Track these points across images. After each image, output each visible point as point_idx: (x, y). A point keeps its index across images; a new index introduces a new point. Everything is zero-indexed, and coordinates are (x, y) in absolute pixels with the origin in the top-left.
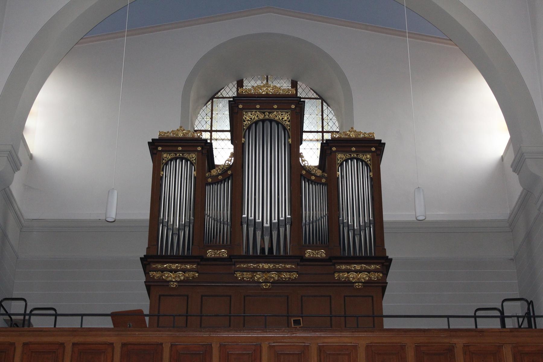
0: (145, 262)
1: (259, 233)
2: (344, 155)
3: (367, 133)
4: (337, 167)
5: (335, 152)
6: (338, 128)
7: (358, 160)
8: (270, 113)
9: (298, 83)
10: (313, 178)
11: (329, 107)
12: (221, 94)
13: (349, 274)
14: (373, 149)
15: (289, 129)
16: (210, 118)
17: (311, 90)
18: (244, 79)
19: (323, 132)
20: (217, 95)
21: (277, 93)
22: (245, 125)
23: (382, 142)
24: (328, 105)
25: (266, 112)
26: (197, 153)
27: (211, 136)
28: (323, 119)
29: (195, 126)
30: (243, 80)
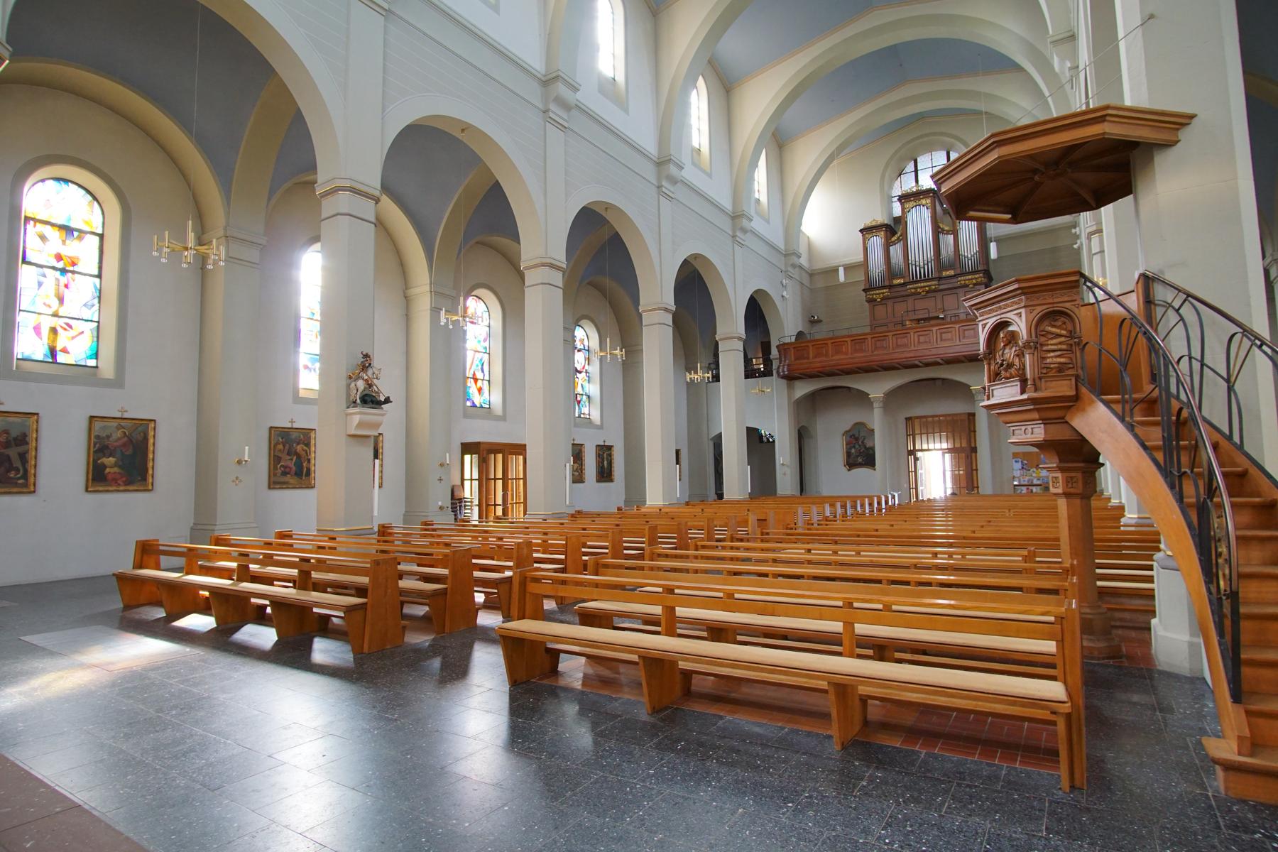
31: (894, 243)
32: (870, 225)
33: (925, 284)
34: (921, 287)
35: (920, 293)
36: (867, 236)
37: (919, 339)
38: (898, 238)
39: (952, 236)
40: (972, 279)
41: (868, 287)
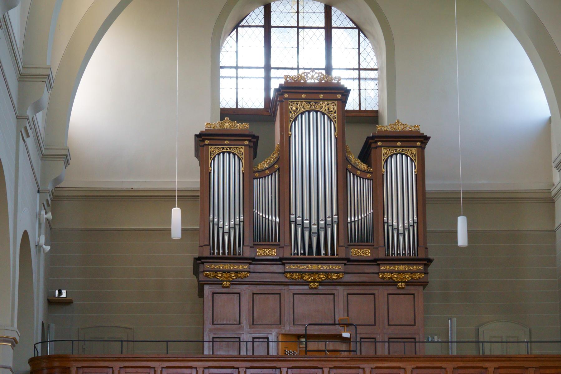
1: (307, 234)
2: (390, 150)
4: (383, 163)
5: (381, 146)
6: (377, 64)
7: (402, 154)
8: (316, 103)
9: (332, 8)
10: (359, 173)
11: (366, 39)
12: (247, 21)
14: (418, 144)
15: (335, 121)
17: (347, 18)
18: (272, 3)
19: (359, 69)
20: (242, 23)
21: (322, 80)
22: (291, 116)
23: (428, 136)
24: (365, 36)
25: (312, 102)
26: (244, 147)
27: (237, 73)
28: (359, 54)
30: (270, 4)
31: (262, 174)
33: (320, 267)
34: (312, 273)
35: (307, 283)
36: (211, 149)
38: (271, 167)
39: (370, 182)
40: (404, 272)
41: (206, 254)
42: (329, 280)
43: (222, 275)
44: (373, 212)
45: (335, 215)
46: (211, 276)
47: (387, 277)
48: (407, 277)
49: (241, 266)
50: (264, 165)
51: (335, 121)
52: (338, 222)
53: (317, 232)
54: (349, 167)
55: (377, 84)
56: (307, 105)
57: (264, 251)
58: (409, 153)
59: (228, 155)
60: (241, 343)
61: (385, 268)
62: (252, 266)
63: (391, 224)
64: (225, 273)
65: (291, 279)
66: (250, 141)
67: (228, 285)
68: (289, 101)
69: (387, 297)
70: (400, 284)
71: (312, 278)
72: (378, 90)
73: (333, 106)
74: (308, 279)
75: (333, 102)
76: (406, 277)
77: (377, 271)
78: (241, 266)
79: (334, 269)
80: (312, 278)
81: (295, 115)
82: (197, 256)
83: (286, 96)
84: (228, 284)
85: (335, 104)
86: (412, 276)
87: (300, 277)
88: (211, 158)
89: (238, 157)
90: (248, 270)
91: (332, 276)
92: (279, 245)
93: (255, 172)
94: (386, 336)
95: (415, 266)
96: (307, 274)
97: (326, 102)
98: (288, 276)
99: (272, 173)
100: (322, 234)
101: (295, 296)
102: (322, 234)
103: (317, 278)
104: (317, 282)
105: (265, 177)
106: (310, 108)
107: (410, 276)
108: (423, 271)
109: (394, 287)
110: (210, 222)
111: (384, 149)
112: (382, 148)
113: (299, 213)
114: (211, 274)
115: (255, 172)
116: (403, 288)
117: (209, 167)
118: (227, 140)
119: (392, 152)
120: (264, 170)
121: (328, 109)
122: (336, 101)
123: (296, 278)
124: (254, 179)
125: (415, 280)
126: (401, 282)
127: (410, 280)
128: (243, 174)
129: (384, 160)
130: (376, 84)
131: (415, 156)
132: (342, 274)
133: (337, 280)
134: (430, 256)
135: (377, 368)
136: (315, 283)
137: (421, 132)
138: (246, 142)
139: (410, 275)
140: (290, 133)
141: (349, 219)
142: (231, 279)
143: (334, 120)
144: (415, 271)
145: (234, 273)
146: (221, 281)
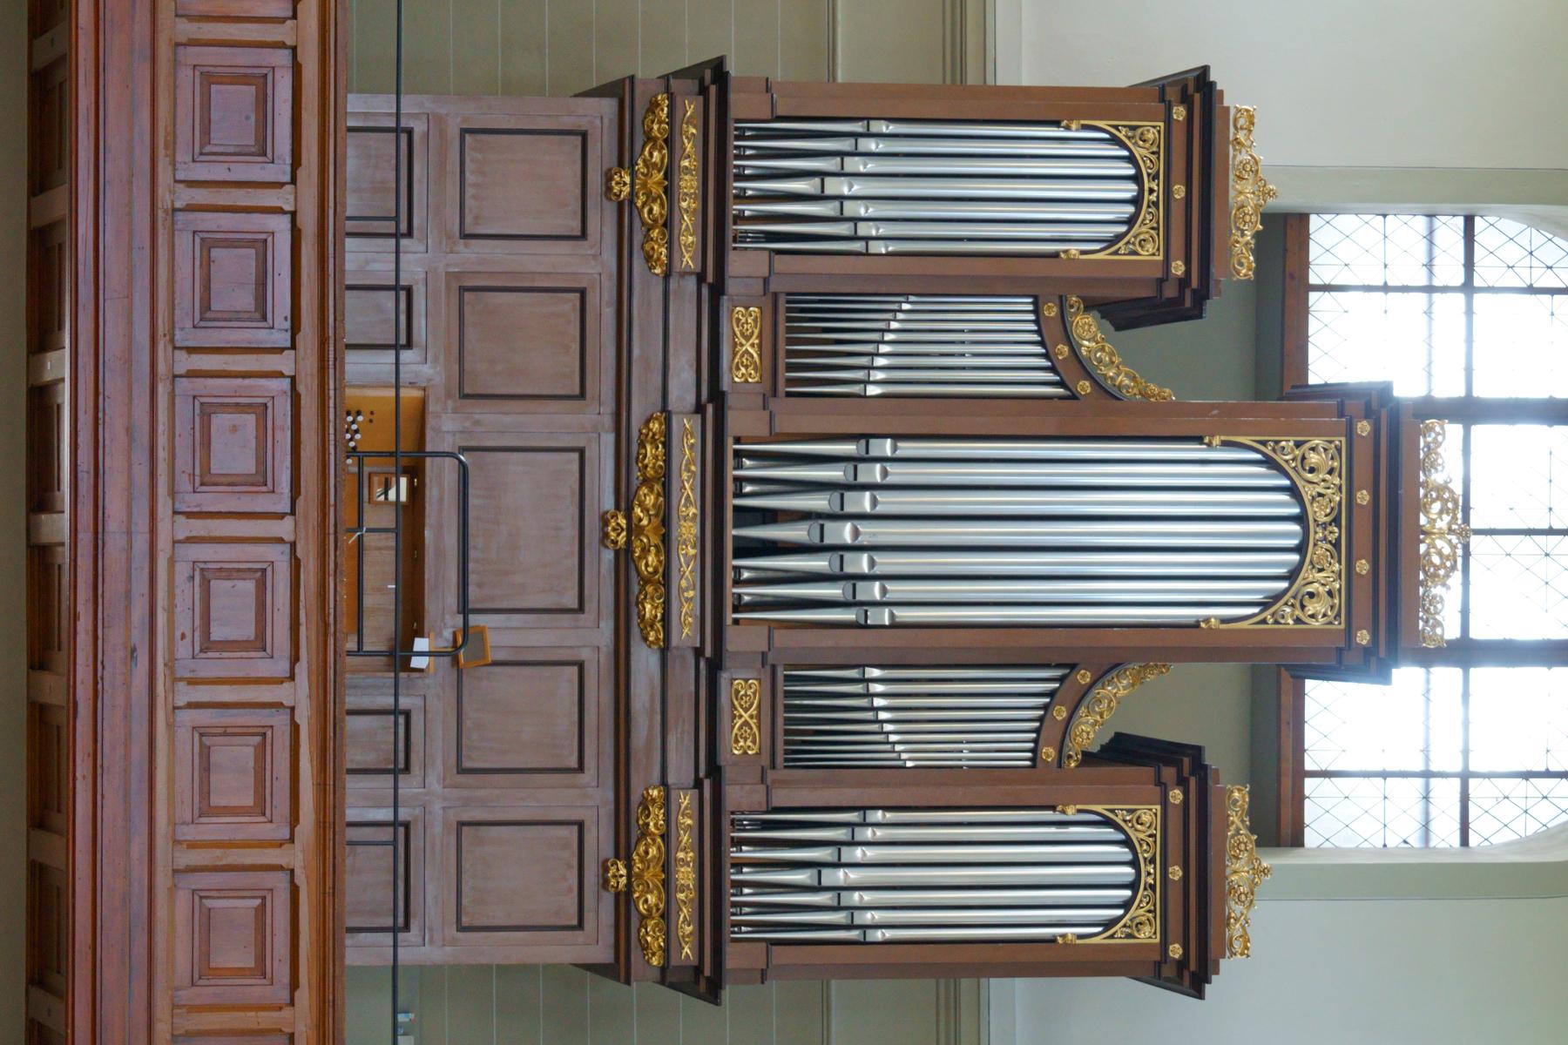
0: (708, 75)
1: (818, 502)
2: (1150, 836)
3: (1248, 930)
4: (1099, 808)
5: (1164, 802)
6: (1486, 843)
7: (1133, 886)
8: (1337, 545)
10: (1061, 713)
13: (659, 840)
16: (1531, 285)
21: (1425, 573)
22: (1283, 448)
23: (1207, 986)
27: (1445, 289)
29: (1491, 219)
32: (1238, 157)
34: (665, 520)
36: (1153, 130)
37: (230, 573)
38: (1082, 366)
40: (667, 884)
41: (740, 105)
42: (635, 588)
43: (655, 164)
44: (905, 767)
45: (892, 615)
46: (653, 122)
47: (648, 816)
48: (649, 897)
49: (691, 239)
50: (1089, 340)
51: (1264, 621)
52: (866, 627)
53: (827, 541)
54: (1083, 676)
55: (1406, 846)
56: (1328, 511)
57: (752, 333)
58: (1138, 912)
59: (1128, 195)
60: (393, 241)
61: (686, 808)
62: (691, 283)
63: (858, 838)
64: (666, 177)
65: (639, 437)
66: (1184, 282)
67: (616, 189)
68: (1343, 439)
69: (573, 818)
70: (623, 871)
71: (645, 522)
72: (1385, 846)
73: (1325, 615)
74: (641, 505)
75: (1338, 615)
76: (647, 892)
77: (671, 780)
78: (691, 239)
79: (682, 605)
80: (645, 522)
81: (1287, 461)
82: (732, 68)
83: (1364, 428)
84: (621, 191)
85: (1331, 623)
86: (653, 918)
87: (650, 472)
88: (1116, 127)
89: (1119, 238)
90: (677, 267)
91: (652, 598)
92: (775, 393)
93: (1062, 302)
94: (418, 811)
95: (691, 928)
96: (661, 499)
97: (1338, 586)
98: (651, 425)
99: (1059, 369)
100: (818, 563)
101: (576, 456)
102: (818, 563)
103: (645, 540)
104: (629, 542)
105: (1042, 343)
106: (1315, 521)
107: (654, 911)
108: (673, 962)
109: (608, 850)
110: (865, 122)
111: (1156, 814)
112: (1158, 807)
113: (898, 473)
114: (660, 122)
115: (1062, 302)
116: (605, 883)
117: (1083, 122)
118: (1187, 192)
119: (1141, 845)
120: (1069, 340)
121: (1311, 595)
122: (1343, 626)
123: (645, 456)
124: (1036, 297)
125: (639, 931)
126: (629, 876)
127: (637, 909)
128: (1056, 255)
129: (1112, 811)
130: (1405, 842)
131: (1130, 936)
132: (661, 637)
133: (635, 620)
134: (727, 993)
135: (295, 728)
136: (624, 533)
137: (1222, 961)
138: (1178, 268)
139: (658, 910)
140: (1216, 441)
141: (875, 673)
142: (639, 204)
143: (1267, 614)
144: (673, 928)
145: (664, 212)
146: (633, 164)
